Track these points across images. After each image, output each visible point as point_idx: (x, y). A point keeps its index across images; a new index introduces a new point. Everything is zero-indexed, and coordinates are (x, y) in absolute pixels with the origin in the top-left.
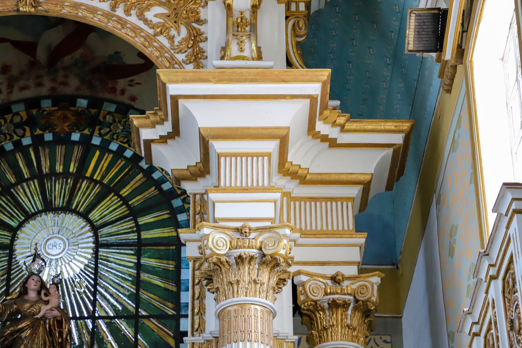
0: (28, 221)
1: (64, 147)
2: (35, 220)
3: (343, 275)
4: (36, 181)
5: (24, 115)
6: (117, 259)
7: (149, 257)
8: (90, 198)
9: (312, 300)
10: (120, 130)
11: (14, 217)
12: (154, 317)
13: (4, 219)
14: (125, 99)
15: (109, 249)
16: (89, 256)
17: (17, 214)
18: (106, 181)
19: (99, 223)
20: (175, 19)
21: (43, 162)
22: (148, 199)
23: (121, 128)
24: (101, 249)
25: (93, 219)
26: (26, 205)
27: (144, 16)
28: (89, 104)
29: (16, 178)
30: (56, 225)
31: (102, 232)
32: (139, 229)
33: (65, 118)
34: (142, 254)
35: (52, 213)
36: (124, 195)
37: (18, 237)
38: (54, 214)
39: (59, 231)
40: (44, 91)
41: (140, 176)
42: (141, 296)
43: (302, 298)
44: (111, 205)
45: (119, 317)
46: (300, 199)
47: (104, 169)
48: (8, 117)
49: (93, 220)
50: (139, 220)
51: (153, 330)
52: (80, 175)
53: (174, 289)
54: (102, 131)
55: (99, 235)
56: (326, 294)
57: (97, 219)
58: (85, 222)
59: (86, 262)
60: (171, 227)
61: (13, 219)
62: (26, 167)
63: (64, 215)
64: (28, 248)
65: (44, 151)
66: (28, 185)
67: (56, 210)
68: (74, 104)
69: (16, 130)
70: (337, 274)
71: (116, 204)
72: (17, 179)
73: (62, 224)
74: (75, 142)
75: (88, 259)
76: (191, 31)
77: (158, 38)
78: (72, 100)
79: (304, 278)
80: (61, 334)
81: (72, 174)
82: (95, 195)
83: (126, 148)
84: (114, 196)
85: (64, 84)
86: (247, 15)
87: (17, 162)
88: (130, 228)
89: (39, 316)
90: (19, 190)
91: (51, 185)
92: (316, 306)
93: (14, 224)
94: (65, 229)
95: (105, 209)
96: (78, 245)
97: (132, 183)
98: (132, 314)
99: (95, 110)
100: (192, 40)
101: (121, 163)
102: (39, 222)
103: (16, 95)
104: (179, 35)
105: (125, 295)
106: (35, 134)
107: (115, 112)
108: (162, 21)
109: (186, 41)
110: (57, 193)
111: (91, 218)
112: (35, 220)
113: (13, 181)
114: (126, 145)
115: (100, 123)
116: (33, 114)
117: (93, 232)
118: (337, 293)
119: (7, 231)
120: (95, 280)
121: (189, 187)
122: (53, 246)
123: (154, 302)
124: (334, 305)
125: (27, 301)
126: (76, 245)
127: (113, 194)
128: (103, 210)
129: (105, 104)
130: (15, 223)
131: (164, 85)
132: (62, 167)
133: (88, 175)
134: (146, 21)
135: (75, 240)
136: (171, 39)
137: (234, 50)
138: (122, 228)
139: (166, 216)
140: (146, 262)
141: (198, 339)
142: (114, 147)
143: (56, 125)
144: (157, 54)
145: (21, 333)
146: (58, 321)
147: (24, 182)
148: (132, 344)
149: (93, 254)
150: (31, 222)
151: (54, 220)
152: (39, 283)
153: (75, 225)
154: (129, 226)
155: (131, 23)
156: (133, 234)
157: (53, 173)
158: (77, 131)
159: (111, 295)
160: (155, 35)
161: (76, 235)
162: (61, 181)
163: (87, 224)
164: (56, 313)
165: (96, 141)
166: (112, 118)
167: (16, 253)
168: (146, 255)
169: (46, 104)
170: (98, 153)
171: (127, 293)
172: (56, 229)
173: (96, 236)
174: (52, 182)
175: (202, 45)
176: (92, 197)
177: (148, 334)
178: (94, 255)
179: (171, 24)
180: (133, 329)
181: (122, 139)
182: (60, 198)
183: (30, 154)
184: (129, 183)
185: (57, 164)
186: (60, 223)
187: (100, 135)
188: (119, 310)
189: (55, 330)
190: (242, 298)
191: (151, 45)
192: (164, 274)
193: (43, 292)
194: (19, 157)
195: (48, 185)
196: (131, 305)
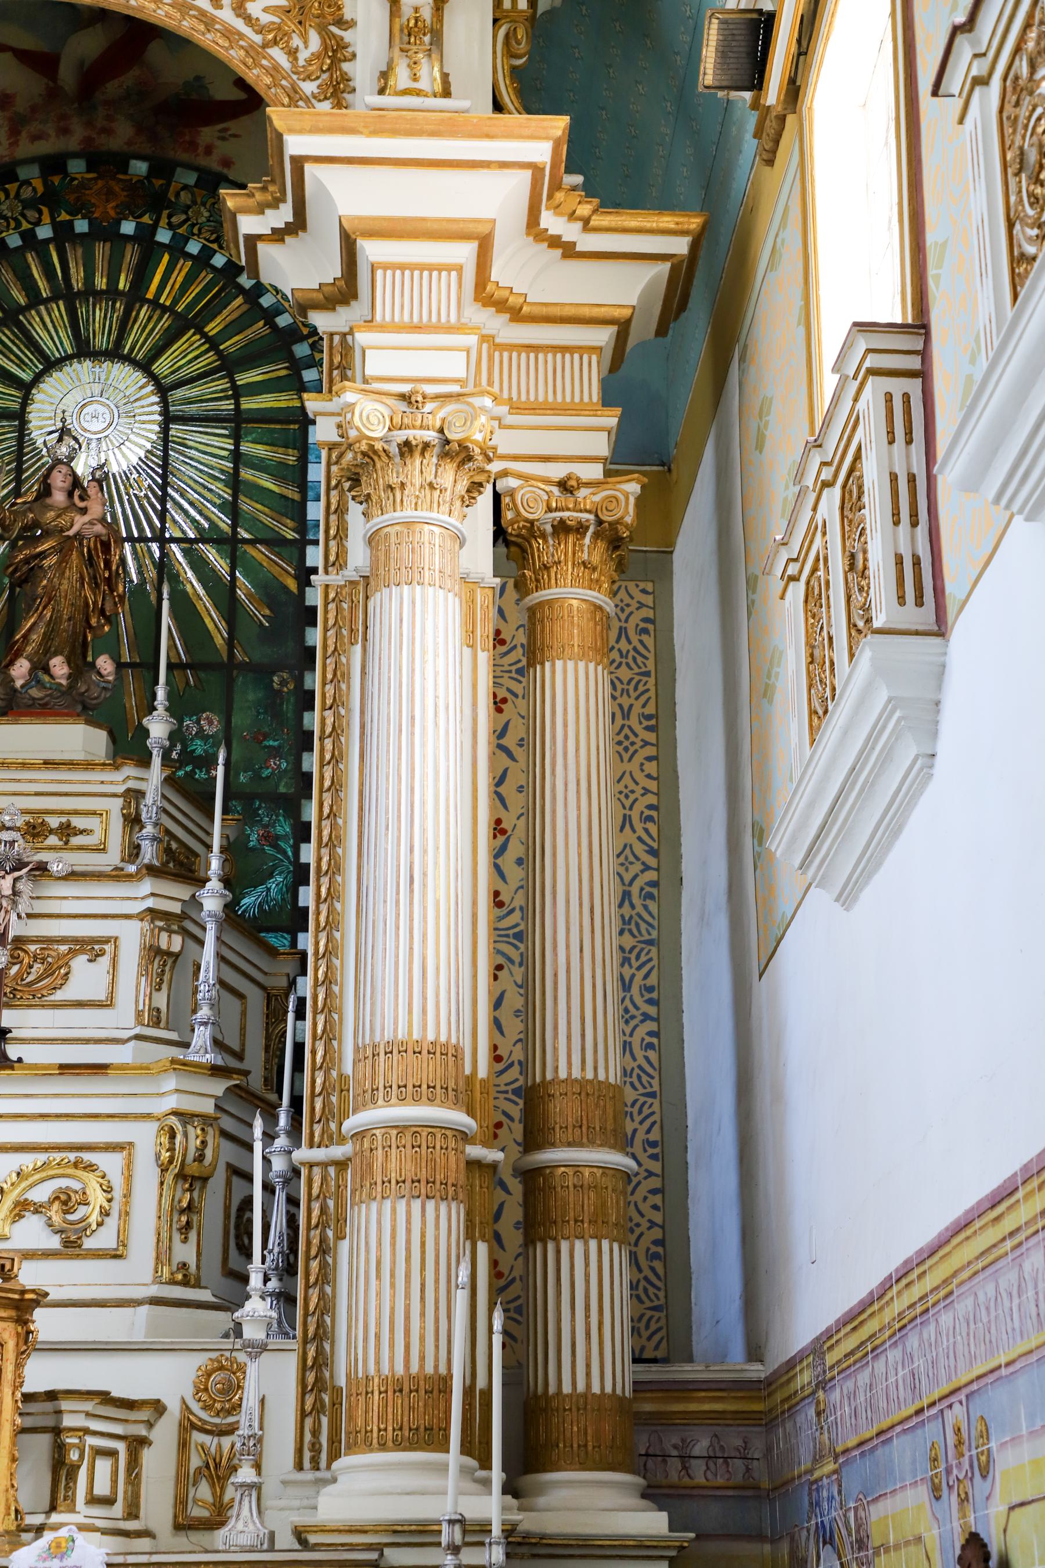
1: (108, 245)
3: (578, 479)
4: (61, 303)
5: (38, 184)
6: (200, 443)
9: (527, 520)
10: (204, 219)
11: (26, 365)
12: (261, 542)
14: (212, 163)
16: (154, 437)
18: (180, 308)
19: (168, 380)
20: (300, 18)
21: (73, 271)
22: (252, 342)
23: (206, 214)
26: (45, 344)
27: (245, 9)
28: (150, 169)
29: (27, 296)
32: (237, 393)
33: (110, 194)
36: (211, 334)
37: (32, 400)
40: (73, 143)
41: (239, 300)
43: (509, 515)
45: (205, 541)
46: (511, 347)
47: (177, 286)
48: (12, 187)
50: (237, 376)
51: (261, 564)
52: (136, 295)
53: (297, 497)
54: (174, 220)
56: (550, 510)
57: (166, 373)
59: (149, 446)
64: (50, 418)
68: (124, 168)
69: (25, 211)
70: (569, 477)
71: (197, 348)
73: (107, 379)
74: (127, 238)
76: (328, 41)
77: (269, 51)
79: (512, 482)
80: (108, 564)
81: (122, 293)
83: (215, 252)
84: (194, 334)
85: (108, 131)
86: (427, 14)
87: (29, 267)
88: (222, 391)
89: (71, 533)
91: (87, 312)
92: (532, 529)
93: (26, 376)
94: (112, 389)
97: (225, 312)
99: (161, 182)
100: (329, 57)
101: (206, 277)
103: (26, 148)
104: (306, 47)
105: (214, 505)
106: (58, 219)
107: (196, 185)
108: (277, 20)
109: (318, 58)
110: (97, 325)
113: (22, 301)
114: (215, 246)
115: (170, 205)
116: (53, 183)
118: (568, 509)
120: (164, 477)
121: (322, 321)
124: (562, 528)
125: (50, 507)
127: (192, 331)
129: (179, 170)
130: (28, 374)
131: (280, 137)
132: (105, 280)
133: (150, 295)
134: (248, 19)
135: (129, 407)
136: (292, 53)
137: (402, 77)
139: (283, 373)
141: (335, 579)
142: (193, 247)
143: (94, 205)
144: (268, 80)
145: (42, 560)
146: (102, 543)
152: (70, 479)
153: (128, 383)
154: (220, 387)
155: (223, 23)
157: (89, 292)
158: (131, 218)
159: (191, 504)
160: (265, 45)
164: (99, 528)
165: (163, 236)
166: (190, 196)
167: (30, 425)
169: (77, 167)
171: (218, 502)
172: (97, 388)
173: (164, 402)
174: (88, 306)
175: (346, 66)
177: (253, 570)
179: (293, 27)
180: (228, 561)
181: (207, 235)
182: (103, 334)
184: (220, 312)
186: (103, 377)
187: (171, 226)
188: (204, 529)
189: (98, 557)
190: (408, 513)
191: (257, 64)
192: (278, 471)
193: (77, 493)
194: (31, 258)
195: (82, 311)
196: (224, 522)
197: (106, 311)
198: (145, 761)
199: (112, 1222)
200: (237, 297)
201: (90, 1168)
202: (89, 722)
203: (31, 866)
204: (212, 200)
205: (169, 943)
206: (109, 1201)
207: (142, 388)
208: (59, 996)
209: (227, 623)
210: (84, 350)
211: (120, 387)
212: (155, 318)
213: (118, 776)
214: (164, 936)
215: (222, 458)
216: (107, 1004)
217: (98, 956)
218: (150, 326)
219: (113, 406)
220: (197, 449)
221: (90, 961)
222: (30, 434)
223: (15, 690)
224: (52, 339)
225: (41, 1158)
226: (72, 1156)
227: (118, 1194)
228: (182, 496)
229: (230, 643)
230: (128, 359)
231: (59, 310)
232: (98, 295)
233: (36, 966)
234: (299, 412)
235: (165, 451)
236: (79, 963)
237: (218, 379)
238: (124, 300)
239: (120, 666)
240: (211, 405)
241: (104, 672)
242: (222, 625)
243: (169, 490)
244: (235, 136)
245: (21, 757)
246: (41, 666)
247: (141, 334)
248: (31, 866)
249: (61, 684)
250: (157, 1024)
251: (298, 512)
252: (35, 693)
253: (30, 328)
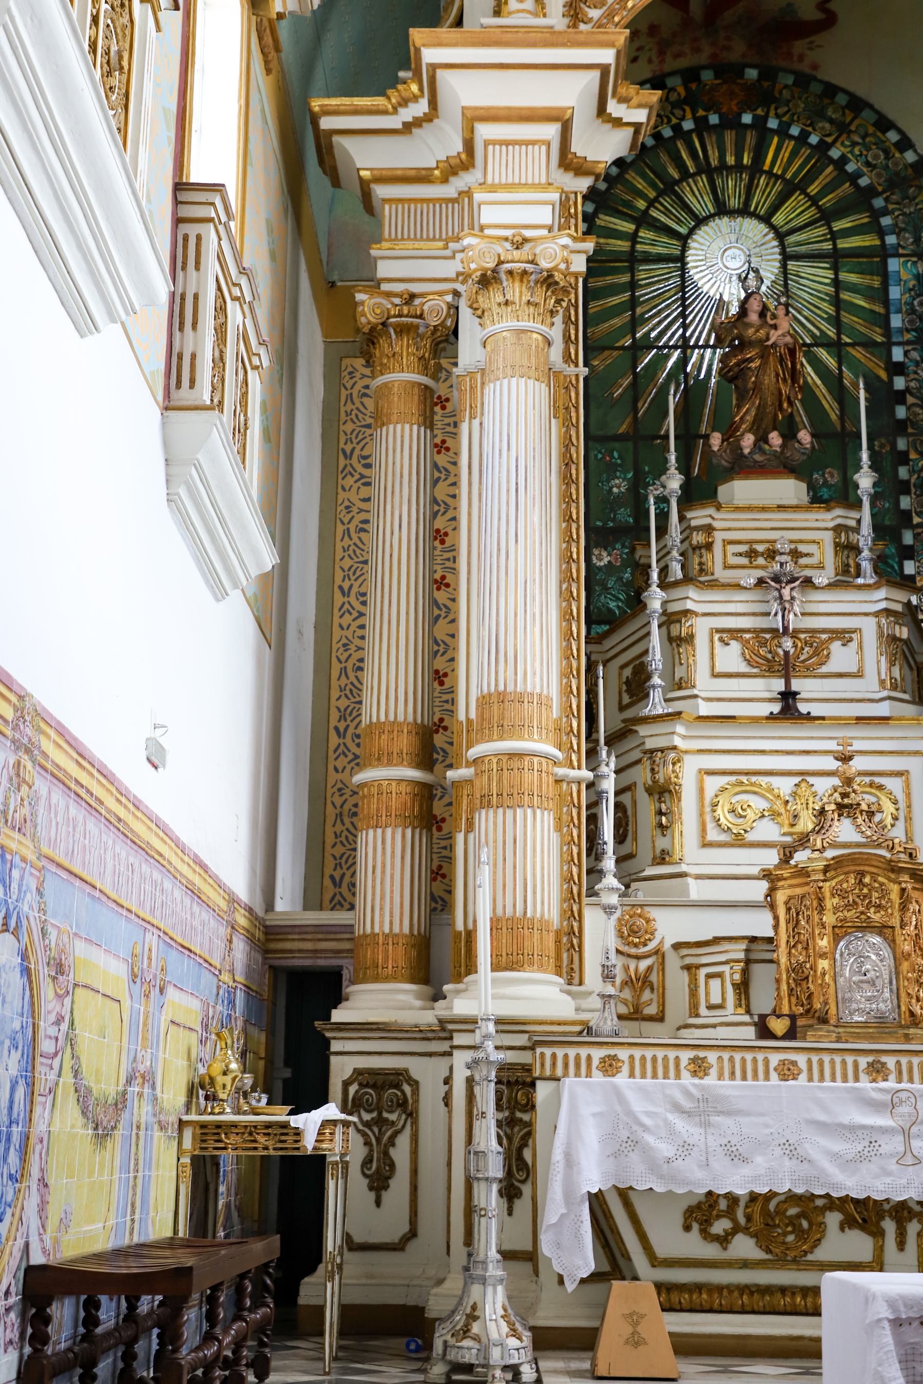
1: (734, 132)
4: (704, 176)
5: (681, 90)
7: (848, 272)
11: (682, 222)
12: (859, 344)
14: (805, 68)
16: (777, 271)
18: (788, 176)
19: (784, 229)
21: (710, 152)
23: (802, 106)
28: (760, 74)
29: (680, 172)
32: (834, 236)
36: (812, 194)
40: (703, 58)
41: (831, 168)
45: (817, 345)
47: (785, 160)
50: (833, 224)
51: (860, 361)
52: (756, 168)
54: (779, 111)
64: (702, 260)
67: (732, 213)
68: (741, 74)
71: (803, 205)
73: (740, 230)
74: (746, 126)
78: (738, 70)
83: (810, 133)
84: (800, 195)
91: (723, 182)
93: (683, 230)
97: (821, 177)
103: (671, 64)
106: (698, 115)
107: (795, 84)
113: (676, 176)
114: (810, 129)
115: (775, 100)
123: (858, 327)
125: (749, 325)
127: (798, 192)
132: (733, 158)
133: (766, 168)
135: (757, 250)
139: (866, 220)
142: (795, 131)
151: (730, 226)
157: (723, 166)
159: (806, 318)
165: (773, 124)
168: (845, 269)
169: (707, 76)
170: (776, 139)
171: (825, 316)
172: (733, 237)
173: (782, 245)
183: (694, 143)
184: (817, 178)
186: (737, 229)
187: (777, 116)
188: (816, 336)
192: (867, 293)
194: (680, 145)
195: (718, 182)
196: (831, 332)
198: (857, 505)
199: (901, 824)
200: (828, 166)
201: (880, 787)
202: (796, 478)
203: (801, 580)
204: (805, 95)
205: (901, 632)
206: (897, 810)
207: (765, 235)
208: (824, 669)
209: (838, 403)
210: (722, 210)
211: (750, 235)
212: (771, 184)
213: (829, 516)
214: (897, 627)
216: (859, 675)
217: (848, 641)
218: (768, 190)
219: (745, 250)
220: (808, 279)
221: (844, 645)
223: (742, 455)
224: (699, 202)
225: (733, 779)
226: (867, 779)
227: (902, 805)
228: (800, 313)
229: (842, 418)
230: (754, 215)
232: (729, 169)
233: (807, 649)
235: (786, 279)
236: (836, 646)
237: (819, 227)
238: (748, 172)
239: (707, 437)
240: (816, 246)
241: (804, 442)
242: (835, 405)
243: (791, 309)
244: (819, 46)
245: (760, 503)
246: (762, 439)
248: (801, 580)
249: (776, 451)
250: (894, 687)
251: (884, 322)
252: (758, 457)
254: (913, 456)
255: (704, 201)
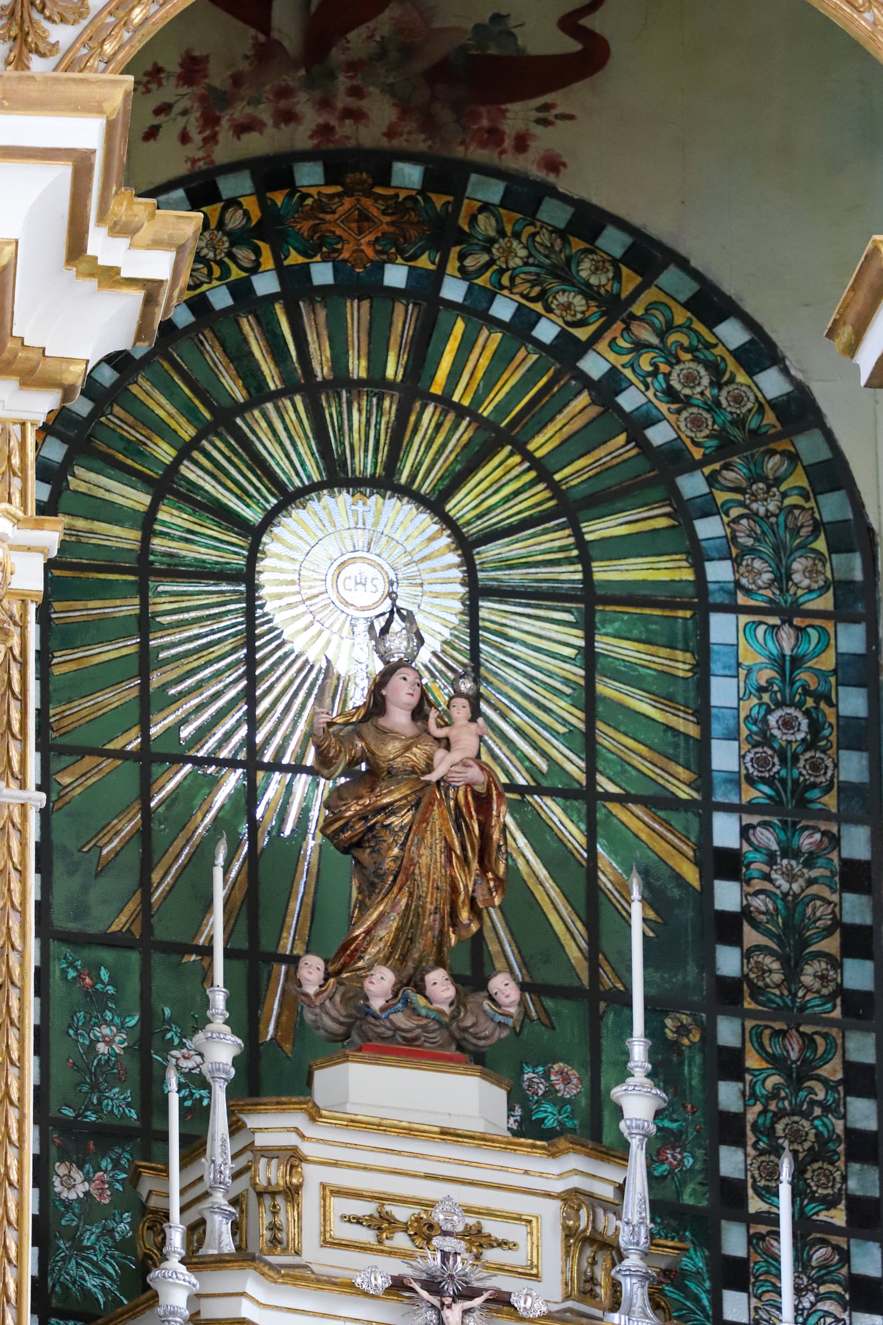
0: (287, 510)
2: (304, 508)
4: (298, 399)
8: (447, 457)
11: (251, 497)
13: (225, 501)
15: (507, 603)
16: (455, 620)
17: (257, 489)
19: (472, 530)
21: (313, 347)
24: (483, 600)
25: (458, 515)
26: (278, 464)
29: (246, 387)
30: (360, 525)
31: (483, 555)
34: (598, 625)
35: (348, 492)
38: (353, 496)
39: (369, 544)
42: (600, 740)
44: (504, 480)
49: (458, 519)
55: (477, 562)
57: (468, 516)
58: (435, 523)
60: (676, 554)
61: (248, 500)
62: (269, 360)
63: (380, 500)
64: (292, 583)
65: (314, 313)
66: (277, 409)
69: (234, 250)
71: (517, 477)
72: (249, 392)
73: (376, 524)
75: (451, 626)
82: (458, 449)
87: (245, 341)
88: (561, 549)
90: (257, 421)
91: (340, 414)
94: (384, 539)
95: (489, 492)
96: (422, 585)
98: (577, 786)
102: (316, 514)
110: (356, 435)
111: (451, 514)
112: (304, 508)
117: (460, 552)
119: (236, 533)
122: (357, 584)
126: (415, 585)
128: (484, 492)
135: (413, 568)
138: (538, 548)
140: (609, 648)
147: (268, 401)
148: (582, 866)
149: (462, 613)
150: (294, 513)
154: (557, 544)
156: (571, 568)
159: (518, 730)
161: (416, 558)
162: (364, 403)
163: (443, 530)
167: (262, 593)
168: (610, 629)
171: (562, 729)
172: (361, 538)
174: (340, 405)
176: (451, 452)
178: (467, 618)
180: (583, 827)
182: (366, 450)
185: (350, 353)
186: (370, 521)
194: (248, 326)
195: (331, 412)
197: (369, 412)
207: (431, 539)
211: (396, 536)
215: (565, 659)
218: (440, 439)
219: (387, 568)
220: (524, 644)
222: (262, 607)
224: (288, 456)
228: (504, 716)
230: (406, 492)
231: (296, 410)
234: (691, 591)
237: (554, 530)
240: (544, 572)
243: (484, 707)
247: (426, 452)
253: (250, 434)
254: (753, 1061)
255: (299, 454)
